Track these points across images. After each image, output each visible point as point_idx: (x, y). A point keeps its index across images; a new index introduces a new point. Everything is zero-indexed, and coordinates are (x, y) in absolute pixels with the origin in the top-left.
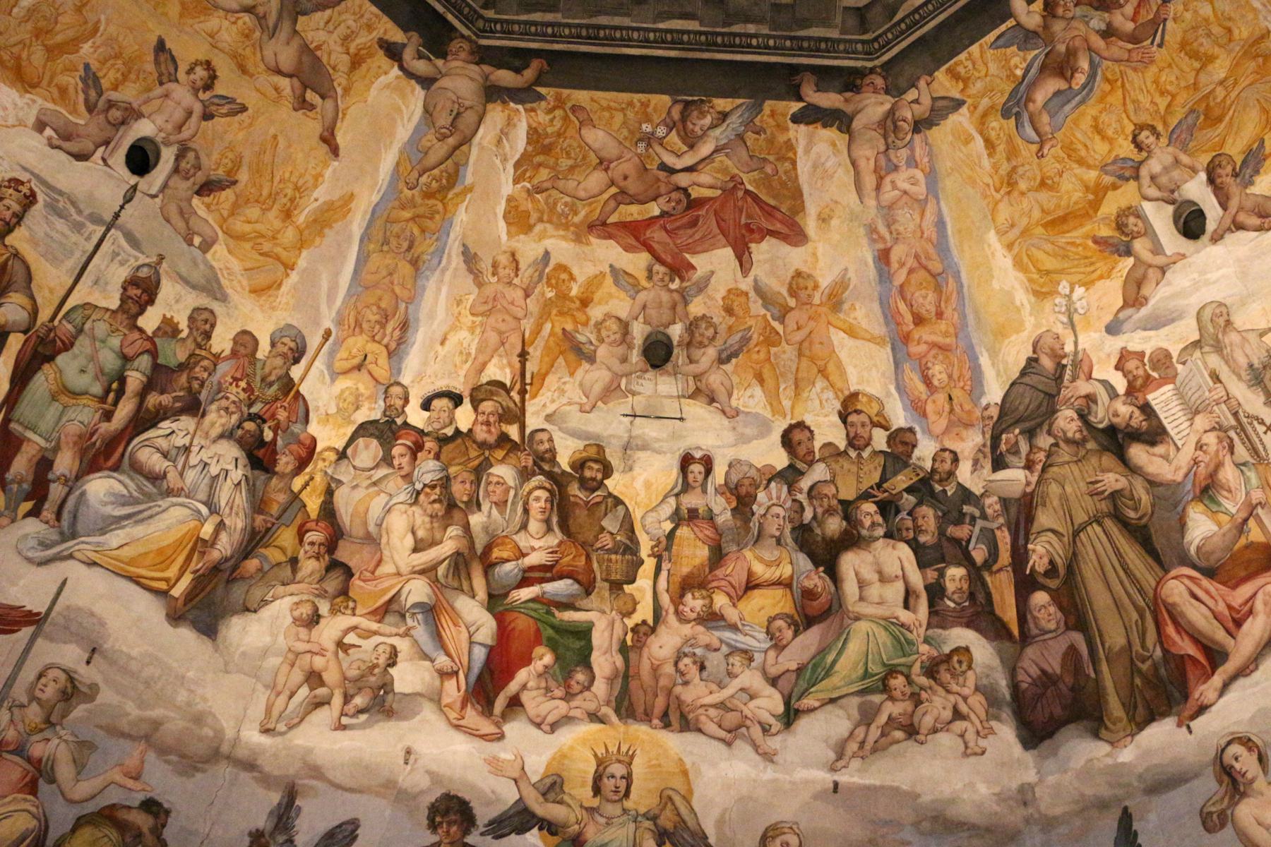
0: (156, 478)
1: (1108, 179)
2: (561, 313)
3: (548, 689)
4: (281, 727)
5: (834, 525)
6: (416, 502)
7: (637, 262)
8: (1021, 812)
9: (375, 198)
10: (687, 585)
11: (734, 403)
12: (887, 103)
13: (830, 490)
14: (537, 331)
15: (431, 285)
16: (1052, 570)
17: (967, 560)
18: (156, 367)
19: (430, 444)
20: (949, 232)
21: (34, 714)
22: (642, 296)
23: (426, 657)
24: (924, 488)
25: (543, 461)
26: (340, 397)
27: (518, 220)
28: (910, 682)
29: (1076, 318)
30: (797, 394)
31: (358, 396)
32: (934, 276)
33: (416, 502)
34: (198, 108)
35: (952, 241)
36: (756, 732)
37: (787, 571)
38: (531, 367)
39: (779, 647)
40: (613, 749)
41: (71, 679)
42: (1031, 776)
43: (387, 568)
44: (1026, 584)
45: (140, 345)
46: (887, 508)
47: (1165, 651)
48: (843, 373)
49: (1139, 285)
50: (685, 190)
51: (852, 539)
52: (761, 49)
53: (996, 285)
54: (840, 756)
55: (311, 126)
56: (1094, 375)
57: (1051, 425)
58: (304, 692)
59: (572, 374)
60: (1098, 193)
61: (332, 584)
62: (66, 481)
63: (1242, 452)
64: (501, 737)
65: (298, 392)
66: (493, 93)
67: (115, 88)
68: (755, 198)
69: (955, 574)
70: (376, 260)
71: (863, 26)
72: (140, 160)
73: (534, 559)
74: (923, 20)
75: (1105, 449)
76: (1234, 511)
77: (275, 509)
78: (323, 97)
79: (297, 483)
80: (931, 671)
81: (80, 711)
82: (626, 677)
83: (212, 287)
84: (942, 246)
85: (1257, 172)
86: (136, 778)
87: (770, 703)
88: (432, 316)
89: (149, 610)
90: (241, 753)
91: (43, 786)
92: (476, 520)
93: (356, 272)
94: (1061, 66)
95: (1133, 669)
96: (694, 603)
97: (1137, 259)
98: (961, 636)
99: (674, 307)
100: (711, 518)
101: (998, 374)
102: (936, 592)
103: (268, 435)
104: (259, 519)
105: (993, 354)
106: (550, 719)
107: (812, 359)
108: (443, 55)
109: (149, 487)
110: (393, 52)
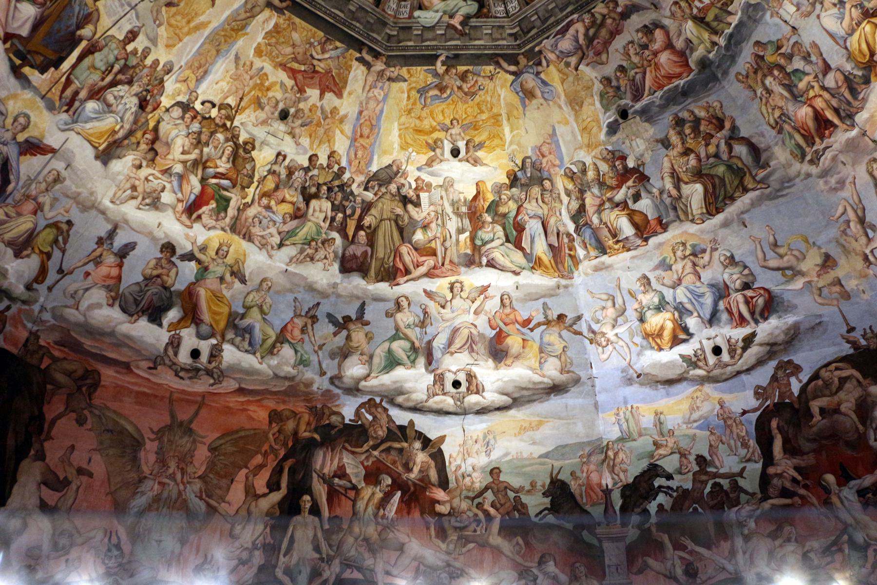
0: (109, 106)
2: (259, 90)
3: (211, 216)
4: (118, 202)
5: (313, 190)
6: (187, 137)
7: (290, 83)
8: (332, 290)
9: (216, 25)
10: (265, 195)
12: (383, 67)
13: (316, 178)
15: (220, 61)
16: (369, 227)
17: (344, 212)
18: (125, 65)
19: (199, 118)
21: (43, 186)
22: (287, 95)
23: (175, 192)
24: (341, 187)
25: (234, 138)
26: (175, 90)
27: (259, 52)
31: (181, 91)
35: (383, 118)
36: (269, 248)
37: (295, 199)
38: (242, 104)
39: (285, 223)
41: (58, 175)
42: (339, 281)
43: (170, 157)
44: (359, 227)
46: (330, 190)
47: (394, 265)
48: (334, 144)
49: (433, 161)
51: (316, 196)
54: (291, 261)
58: (129, 192)
60: (434, 130)
61: (150, 156)
63: (439, 221)
64: (191, 227)
65: (163, 86)
68: (334, 78)
69: (340, 215)
70: (206, 46)
73: (220, 170)
75: (401, 201)
79: (150, 115)
80: (323, 243)
81: (58, 187)
82: (237, 219)
83: (154, 41)
84: (379, 118)
86: (67, 212)
87: (277, 240)
88: (216, 73)
89: (90, 152)
90: (101, 207)
91: (39, 213)
92: (206, 150)
94: (442, 89)
95: (382, 265)
96: (265, 201)
97: (436, 154)
98: (335, 235)
100: (279, 175)
102: (333, 219)
103: (148, 98)
107: (328, 136)
109: (106, 108)
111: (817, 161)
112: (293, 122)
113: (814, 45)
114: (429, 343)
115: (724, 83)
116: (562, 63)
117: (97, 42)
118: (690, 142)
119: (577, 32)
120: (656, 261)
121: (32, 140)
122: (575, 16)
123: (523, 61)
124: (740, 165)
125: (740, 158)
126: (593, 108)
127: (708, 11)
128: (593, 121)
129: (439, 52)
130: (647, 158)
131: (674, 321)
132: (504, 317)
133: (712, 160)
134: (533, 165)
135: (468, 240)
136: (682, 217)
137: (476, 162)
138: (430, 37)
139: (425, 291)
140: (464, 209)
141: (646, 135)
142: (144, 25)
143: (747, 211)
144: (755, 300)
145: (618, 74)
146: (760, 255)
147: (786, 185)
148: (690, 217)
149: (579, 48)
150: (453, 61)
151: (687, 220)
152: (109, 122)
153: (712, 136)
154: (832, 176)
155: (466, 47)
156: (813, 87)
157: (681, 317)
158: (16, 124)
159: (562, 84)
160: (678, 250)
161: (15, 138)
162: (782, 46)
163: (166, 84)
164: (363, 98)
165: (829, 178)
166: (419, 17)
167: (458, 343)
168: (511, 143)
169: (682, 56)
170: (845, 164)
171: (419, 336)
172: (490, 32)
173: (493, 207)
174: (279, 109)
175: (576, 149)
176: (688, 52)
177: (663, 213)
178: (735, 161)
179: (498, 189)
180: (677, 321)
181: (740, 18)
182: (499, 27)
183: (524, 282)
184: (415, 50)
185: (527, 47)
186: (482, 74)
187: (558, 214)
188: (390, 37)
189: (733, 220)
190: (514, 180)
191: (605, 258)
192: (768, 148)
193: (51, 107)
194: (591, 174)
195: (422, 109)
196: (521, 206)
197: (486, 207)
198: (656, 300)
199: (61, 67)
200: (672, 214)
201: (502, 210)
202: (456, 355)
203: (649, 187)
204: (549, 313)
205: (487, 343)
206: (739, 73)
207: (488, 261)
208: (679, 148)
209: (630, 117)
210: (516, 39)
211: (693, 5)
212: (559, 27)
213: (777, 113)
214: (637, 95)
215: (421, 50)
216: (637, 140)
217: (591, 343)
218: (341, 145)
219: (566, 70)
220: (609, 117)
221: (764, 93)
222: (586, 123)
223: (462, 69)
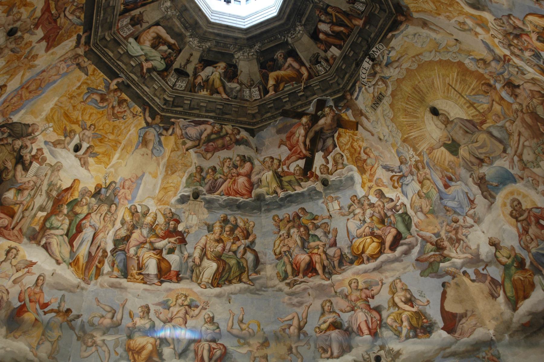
7: (38, 13)
20: (54, 85)
22: (29, 20)
29: (45, 132)
30: (4, 73)
32: (40, 86)
35: (51, 87)
49: (59, 144)
50: (59, 17)
52: (97, 20)
53: (45, 105)
56: (33, 145)
57: (15, 140)
59: (3, 12)
60: (76, 122)
75: (16, 158)
76: (19, 199)
84: (49, 84)
94: (103, 99)
97: (65, 140)
99: (26, 30)
101: (21, 117)
107: (14, 71)
111: (292, 285)
112: (11, 43)
113: (336, 231)
115: (263, 215)
116: (181, 140)
118: (225, 236)
119: (205, 130)
120: (162, 299)
123: (158, 119)
124: (245, 265)
125: (247, 261)
126: (180, 179)
127: (288, 175)
128: (174, 187)
130: (193, 231)
131: (154, 346)
132: (32, 294)
133: (231, 253)
135: (42, 219)
136: (194, 278)
137: (84, 164)
138: (125, 61)
140: (54, 194)
141: (202, 217)
143: (235, 294)
144: (215, 350)
145: (210, 171)
146: (230, 324)
147: (263, 289)
148: (199, 281)
150: (124, 87)
151: (196, 282)
153: (239, 240)
154: (297, 298)
155: (137, 85)
156: (319, 249)
157: (160, 345)
159: (172, 151)
160: (180, 298)
162: (317, 220)
164: (54, 63)
165: (293, 298)
166: (130, 43)
168: (111, 167)
169: (252, 185)
170: (309, 295)
172: (156, 87)
173: (74, 204)
174: (15, 26)
175: (149, 197)
176: (256, 186)
177: (183, 270)
178: (243, 261)
179: (85, 193)
180: (156, 346)
181: (304, 191)
182: (164, 89)
183: (60, 272)
184: (110, 61)
187: (107, 232)
188: (104, 38)
189: (224, 295)
190: (97, 193)
191: (124, 281)
194: (149, 219)
197: (69, 201)
198: (148, 326)
200: (189, 273)
201: (78, 209)
203: (183, 248)
204: (63, 304)
205: (9, 311)
206: (278, 216)
207: (46, 243)
208: (216, 236)
209: (199, 199)
210: (165, 104)
211: (281, 166)
212: (197, 119)
213: (285, 249)
214: (212, 190)
215: (113, 64)
216: (194, 216)
217: (78, 340)
219: (180, 146)
221: (285, 234)
222: (168, 185)
223: (124, 96)
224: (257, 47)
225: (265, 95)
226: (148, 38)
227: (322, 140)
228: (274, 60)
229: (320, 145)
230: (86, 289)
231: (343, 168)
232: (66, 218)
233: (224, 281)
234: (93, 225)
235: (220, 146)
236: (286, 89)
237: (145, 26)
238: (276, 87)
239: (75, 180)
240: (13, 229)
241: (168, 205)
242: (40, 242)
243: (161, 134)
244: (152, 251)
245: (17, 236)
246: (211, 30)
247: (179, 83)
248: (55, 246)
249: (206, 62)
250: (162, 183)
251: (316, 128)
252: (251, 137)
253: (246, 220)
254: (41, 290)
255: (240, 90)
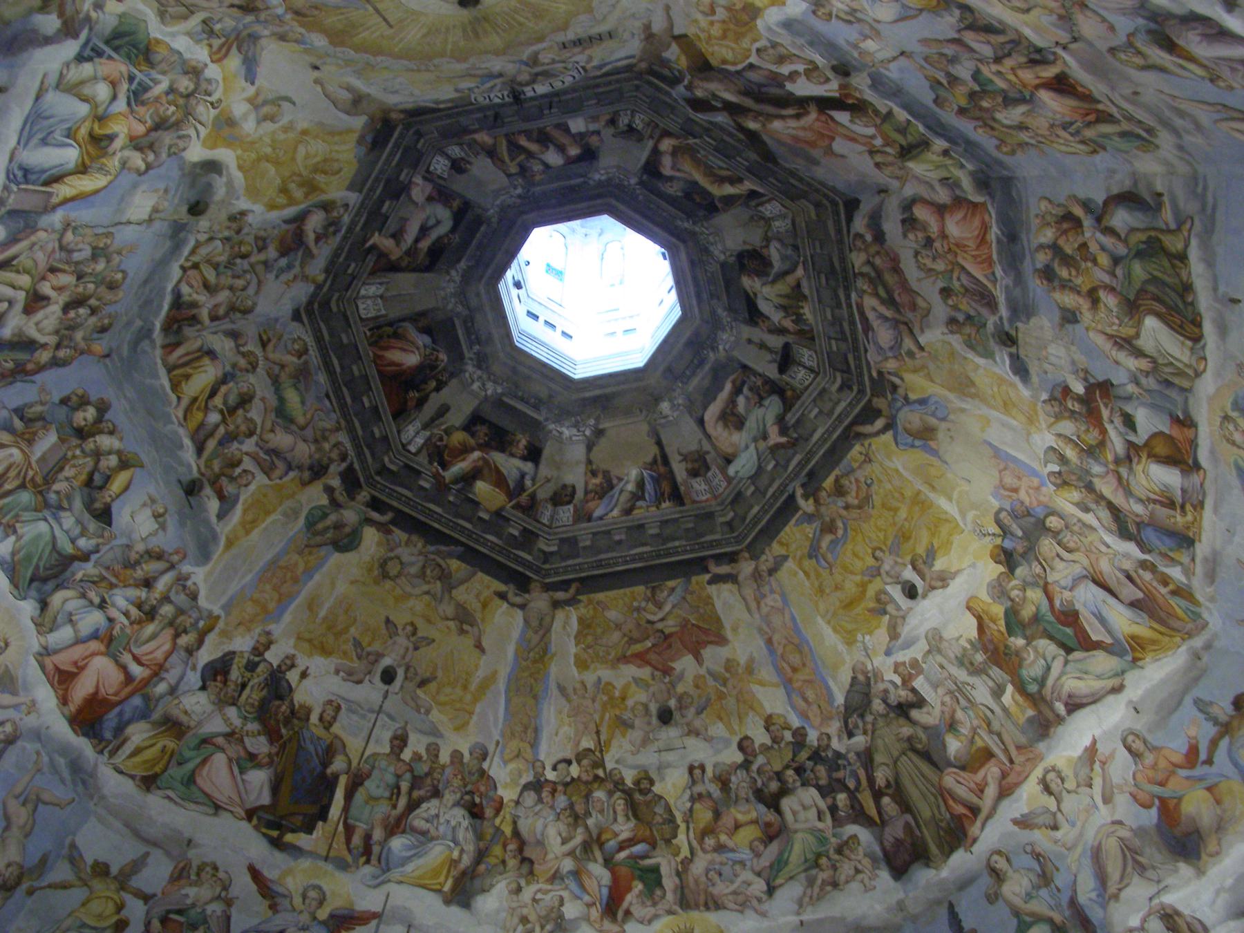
0: (424, 833)
1: (866, 579)
2: (613, 707)
3: (643, 903)
5: (774, 786)
6: (558, 819)
7: (645, 673)
9: (508, 670)
11: (710, 733)
14: (602, 718)
15: (545, 706)
16: (888, 785)
19: (560, 788)
22: (652, 689)
23: (578, 898)
24: (816, 756)
25: (618, 784)
27: (582, 665)
28: (829, 858)
32: (797, 646)
33: (558, 819)
34: (411, 646)
35: (801, 626)
36: (755, 903)
37: (754, 815)
38: (603, 738)
39: (758, 855)
40: (682, 927)
42: (901, 895)
43: (551, 856)
44: (877, 795)
45: (405, 768)
46: (800, 771)
50: (662, 632)
51: (784, 791)
52: (685, 552)
53: (827, 644)
54: (801, 905)
55: (469, 641)
58: (520, 928)
59: (624, 736)
60: (863, 586)
62: (380, 843)
63: (963, 702)
66: (556, 604)
67: (369, 645)
68: (698, 627)
69: (842, 798)
71: (732, 529)
72: (388, 676)
73: (625, 835)
74: (760, 520)
75: (899, 715)
77: (488, 837)
78: (472, 626)
79: (497, 821)
80: (839, 851)
82: (682, 888)
83: (435, 732)
85: (934, 559)
87: (759, 886)
89: (434, 901)
92: (590, 822)
93: (506, 709)
94: (829, 528)
96: (710, 842)
98: (852, 829)
99: (669, 692)
100: (709, 795)
102: (833, 809)
103: (477, 800)
104: (482, 844)
105: (834, 678)
106: (648, 917)
107: (745, 702)
108: (528, 591)
109: (422, 839)
110: (502, 596)
113: (925, 42)
114: (1073, 902)
117: (359, 770)
119: (874, 309)
121: (338, 912)
122: (854, 296)
124: (1143, 237)
125: (1133, 230)
126: (981, 371)
129: (790, 489)
132: (1150, 773)
133: (1119, 271)
134: (1015, 515)
135: (1018, 697)
139: (1016, 822)
140: (979, 657)
141: (1048, 333)
142: (406, 723)
145: (950, 302)
147: (1199, 190)
148: (1191, 372)
149: (896, 324)
150: (812, 484)
151: (1192, 379)
152: (437, 853)
153: (1084, 246)
155: (811, 454)
158: (307, 901)
159: (932, 381)
160: (1231, 434)
161: (315, 918)
163: (491, 773)
166: (737, 472)
167: (1113, 870)
168: (964, 517)
169: (959, 202)
171: (1053, 903)
172: (816, 411)
175: (1028, 441)
176: (958, 192)
177: (1168, 405)
179: (999, 590)
181: (896, 104)
183: (1140, 692)
184: (766, 512)
185: (867, 383)
186: (855, 465)
187: (1103, 549)
188: (730, 525)
190: (1008, 559)
191: (1202, 549)
192: (1135, 179)
193: (343, 866)
194: (1070, 453)
195: (831, 574)
196: (1046, 584)
197: (1003, 629)
199: (330, 816)
200: (1174, 394)
201: (1027, 612)
202: (1123, 895)
203: (1121, 392)
204: (1215, 710)
206: (998, 148)
207: (1066, 705)
208: (1085, 305)
210: (850, 388)
212: (859, 326)
214: (992, 304)
215: (771, 506)
218: (773, 701)
219: (918, 363)
220: (1003, 362)
223: (828, 483)
224: (686, 225)
225: (761, 195)
226: (727, 439)
227: (764, 90)
228: (688, 195)
229: (774, 91)
230: (1215, 636)
231: (782, 45)
232: (1034, 643)
233: (1184, 302)
234: (1074, 580)
235: (896, 278)
236: (724, 166)
237: (707, 446)
238: (733, 181)
239: (969, 608)
240: (1011, 762)
241: (1035, 405)
242: (1058, 716)
243: (906, 398)
244: (1134, 465)
245: (1028, 760)
246: (696, 310)
247: (805, 360)
248: (1080, 684)
249: (753, 315)
250: (997, 409)
251: (748, 102)
252: (862, 206)
253: (1038, 221)
254: (1154, 749)
255: (780, 240)
